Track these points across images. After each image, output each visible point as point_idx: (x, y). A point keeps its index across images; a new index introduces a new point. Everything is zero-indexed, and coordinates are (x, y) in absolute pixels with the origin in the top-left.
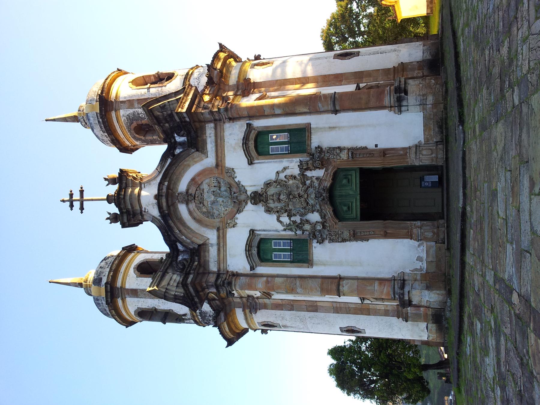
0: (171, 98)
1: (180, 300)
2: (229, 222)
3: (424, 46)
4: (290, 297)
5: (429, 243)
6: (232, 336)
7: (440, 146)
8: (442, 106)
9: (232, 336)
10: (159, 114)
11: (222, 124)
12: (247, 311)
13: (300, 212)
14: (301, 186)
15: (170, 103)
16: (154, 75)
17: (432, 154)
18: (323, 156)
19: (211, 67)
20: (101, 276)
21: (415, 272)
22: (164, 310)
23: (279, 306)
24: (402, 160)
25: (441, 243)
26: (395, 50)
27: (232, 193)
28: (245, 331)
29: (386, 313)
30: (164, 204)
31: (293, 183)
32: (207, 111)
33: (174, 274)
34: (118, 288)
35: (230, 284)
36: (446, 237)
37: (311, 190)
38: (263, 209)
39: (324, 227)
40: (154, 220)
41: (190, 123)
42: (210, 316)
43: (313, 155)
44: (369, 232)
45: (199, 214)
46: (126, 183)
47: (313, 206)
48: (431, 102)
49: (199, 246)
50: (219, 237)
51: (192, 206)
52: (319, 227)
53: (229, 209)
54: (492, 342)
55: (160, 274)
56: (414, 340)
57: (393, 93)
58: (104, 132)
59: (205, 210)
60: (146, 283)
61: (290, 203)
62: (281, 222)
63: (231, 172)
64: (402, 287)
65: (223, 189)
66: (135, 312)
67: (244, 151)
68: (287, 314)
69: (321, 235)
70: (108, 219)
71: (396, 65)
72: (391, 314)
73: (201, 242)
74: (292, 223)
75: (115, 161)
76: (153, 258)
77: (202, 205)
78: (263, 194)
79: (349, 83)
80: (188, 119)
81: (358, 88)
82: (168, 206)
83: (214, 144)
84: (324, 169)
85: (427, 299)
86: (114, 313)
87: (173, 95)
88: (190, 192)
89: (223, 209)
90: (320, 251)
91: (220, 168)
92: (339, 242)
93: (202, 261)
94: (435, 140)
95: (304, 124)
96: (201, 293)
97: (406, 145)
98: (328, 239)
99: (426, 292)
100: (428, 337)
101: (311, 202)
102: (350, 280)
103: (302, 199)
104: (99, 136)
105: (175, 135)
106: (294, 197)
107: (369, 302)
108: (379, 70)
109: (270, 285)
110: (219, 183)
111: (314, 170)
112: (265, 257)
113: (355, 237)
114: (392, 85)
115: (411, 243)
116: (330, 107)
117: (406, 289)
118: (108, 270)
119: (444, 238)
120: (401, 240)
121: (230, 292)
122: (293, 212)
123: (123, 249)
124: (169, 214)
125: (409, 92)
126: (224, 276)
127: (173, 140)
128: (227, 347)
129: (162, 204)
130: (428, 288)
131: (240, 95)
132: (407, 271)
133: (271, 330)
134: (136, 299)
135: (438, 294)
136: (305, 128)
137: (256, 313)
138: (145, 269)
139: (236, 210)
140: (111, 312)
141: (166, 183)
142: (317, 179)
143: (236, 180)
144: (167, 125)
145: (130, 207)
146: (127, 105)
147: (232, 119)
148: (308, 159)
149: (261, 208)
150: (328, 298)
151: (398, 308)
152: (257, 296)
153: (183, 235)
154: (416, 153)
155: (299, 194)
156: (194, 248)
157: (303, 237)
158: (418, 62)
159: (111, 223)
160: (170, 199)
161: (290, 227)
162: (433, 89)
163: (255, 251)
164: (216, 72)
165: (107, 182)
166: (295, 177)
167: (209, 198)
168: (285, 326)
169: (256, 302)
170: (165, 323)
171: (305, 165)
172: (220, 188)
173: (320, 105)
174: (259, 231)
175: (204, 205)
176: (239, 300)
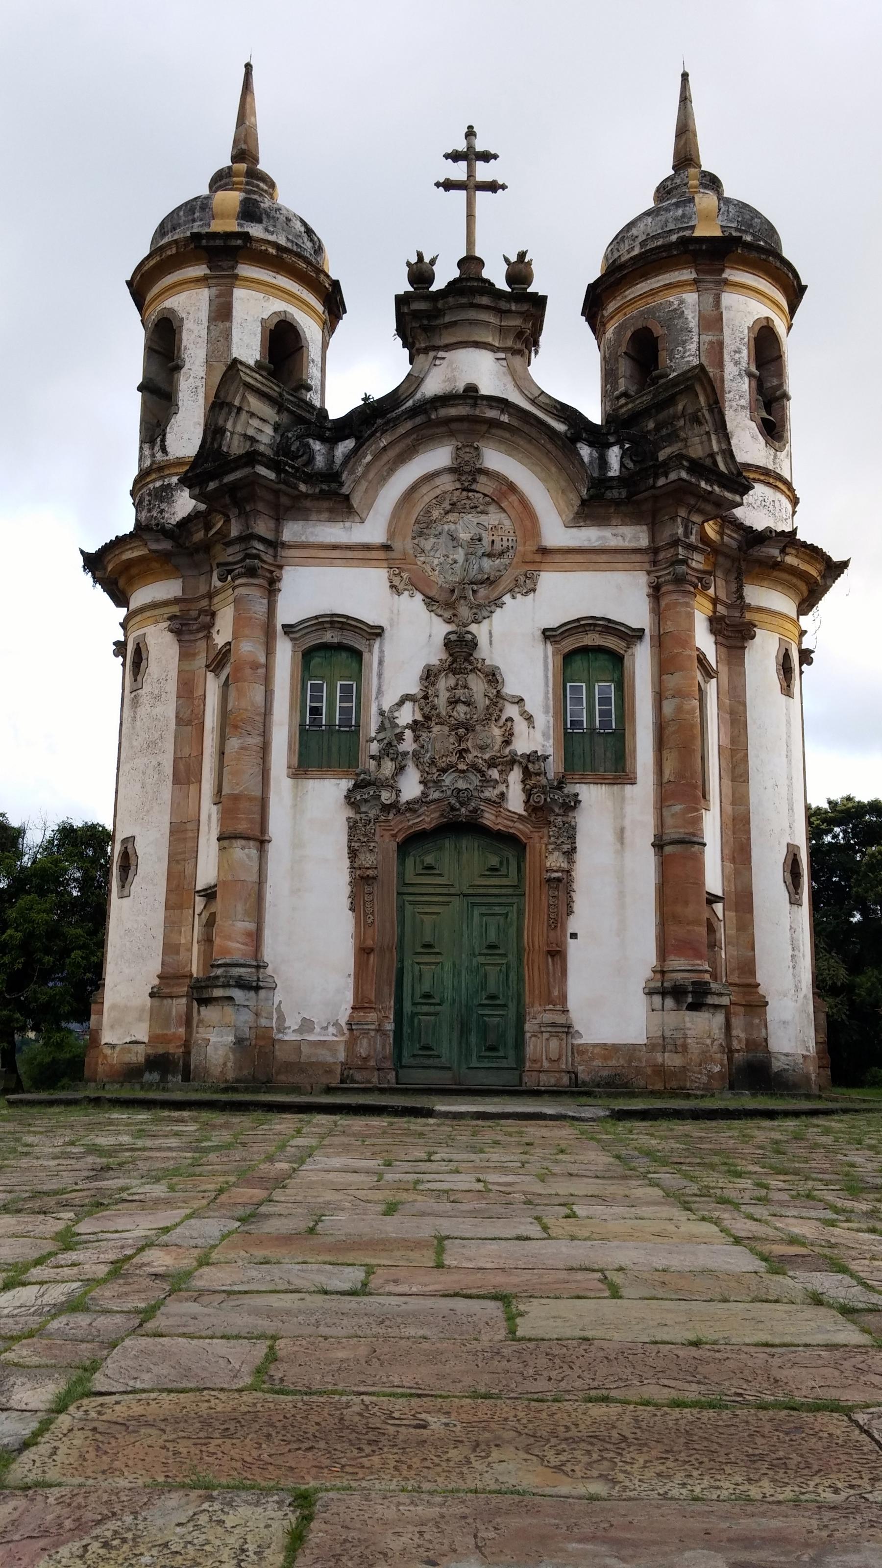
0: (719, 442)
1: (212, 443)
2: (405, 575)
3: (804, 1057)
4: (211, 720)
5: (341, 1048)
6: (110, 568)
7: (565, 1080)
8: (659, 1086)
9: (110, 568)
10: (680, 407)
11: (647, 566)
12: (175, 610)
13: (423, 752)
14: (486, 757)
15: (705, 438)
16: (781, 385)
17: (550, 1060)
18: (557, 810)
19: (789, 539)
20: (265, 220)
21: (275, 1016)
22: (177, 391)
23: (188, 691)
24: (537, 992)
25: (342, 1074)
26: (797, 989)
27: (475, 587)
28: (120, 598)
29: (170, 948)
30: (453, 412)
31: (493, 737)
32: (680, 531)
33: (276, 427)
34: (233, 268)
35: (252, 572)
36: (356, 1086)
37: (476, 780)
38: (434, 661)
39: (386, 808)
40: (413, 381)
41: (654, 487)
42: (162, 511)
43: (560, 788)
44: (372, 914)
45: (427, 499)
46: (509, 311)
47: (437, 783)
48: (668, 1062)
49: (347, 498)
50: (367, 547)
51: (447, 483)
52: (386, 796)
53: (436, 577)
55: (274, 389)
56: (101, 1013)
57: (694, 977)
58: (643, 244)
59: (436, 514)
60: (248, 347)
61: (446, 729)
62: (401, 703)
63: (526, 585)
64: (242, 984)
65: (487, 563)
66: (172, 311)
67: (578, 620)
68: (168, 709)
69: (366, 801)
70: (420, 256)
71: (761, 990)
72: (168, 959)
74: (398, 730)
75: (564, 282)
76: (311, 365)
77: (448, 507)
78: (471, 663)
80: (661, 482)
81: (712, 899)
82: (448, 421)
83: (596, 544)
84: (524, 813)
85: (213, 1039)
86: (169, 253)
87: (724, 447)
88: (482, 479)
89: (436, 562)
90: (329, 794)
91: (538, 558)
92: (350, 841)
93: (308, 503)
94: (580, 1068)
95: (635, 768)
96: (227, 500)
97: (573, 1003)
98: (358, 817)
99: (231, 1038)
100: (113, 1047)
101: (448, 779)
102: (257, 864)
103: (454, 759)
104: (634, 231)
105: (627, 446)
106: (460, 739)
107: (199, 908)
108: (753, 949)
109: (248, 671)
110: (501, 554)
111: (524, 790)
112: (316, 661)
113: (362, 882)
114: (715, 976)
115: (343, 1007)
116: (672, 833)
117: (238, 994)
118: (282, 241)
119: (353, 1081)
120: (351, 986)
121: (230, 572)
122: (424, 735)
123: (336, 284)
124: (430, 424)
125: (695, 1013)
126: (268, 558)
127: (612, 439)
128: (82, 552)
129: (453, 406)
130: (239, 1042)
131: (715, 612)
132: (279, 996)
133: (124, 665)
134: (204, 315)
135: (225, 1064)
136: (624, 771)
137: (171, 631)
138: (283, 340)
139: (432, 593)
140: (169, 244)
141: (505, 418)
142: (502, 795)
143: (507, 598)
144: (651, 425)
145: (447, 319)
146: (709, 309)
147: (656, 592)
148: (551, 775)
149: (435, 655)
150: (209, 814)
151: (185, 977)
152: (215, 636)
153: (376, 457)
154: (554, 1025)
155: (467, 751)
156: (342, 484)
157: (363, 757)
158: (766, 1040)
159: (409, 264)
160: (465, 426)
161: (387, 725)
162: (697, 1069)
163: (330, 637)
164: (775, 552)
165: (513, 259)
166: (507, 742)
167: (465, 527)
168: (135, 703)
169: (198, 631)
170: (140, 388)
171: (537, 767)
172: (489, 555)
173: (678, 808)
174: (382, 651)
175: (447, 513)
176: (203, 589)
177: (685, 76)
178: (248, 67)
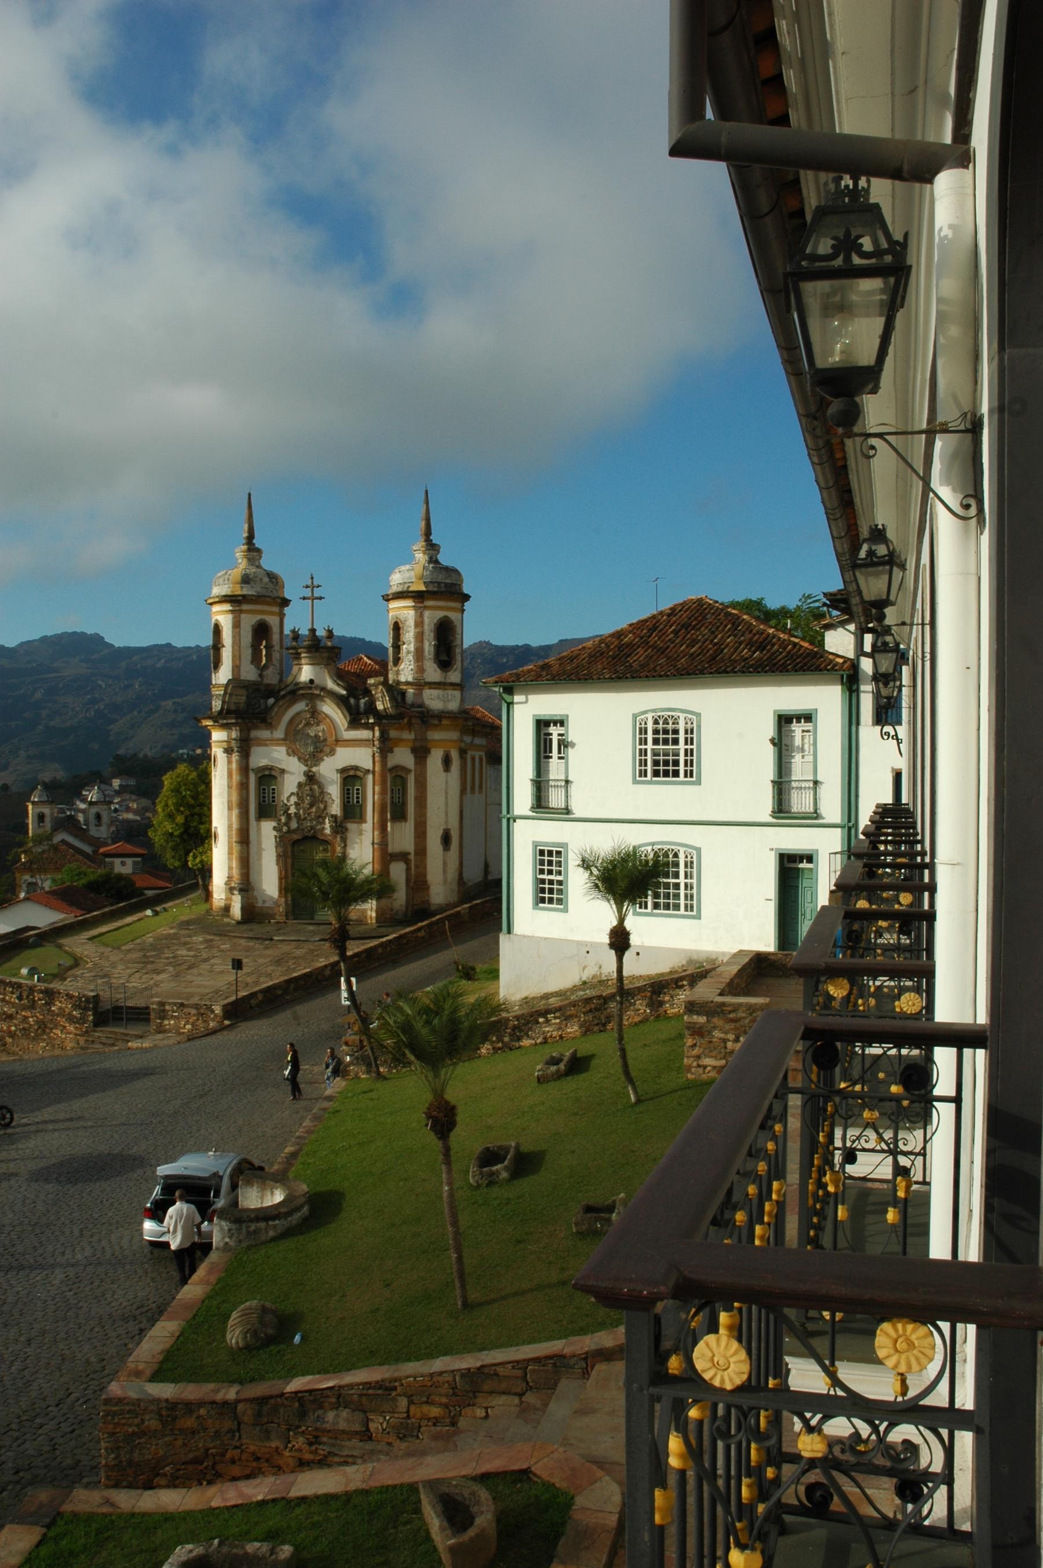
12: (225, 745)
16: (452, 642)
26: (445, 881)
54: (192, 953)
73: (274, 723)
79: (416, 844)
118: (259, 589)
130: (243, 909)
134: (230, 626)
177: (427, 492)
178: (249, 495)
